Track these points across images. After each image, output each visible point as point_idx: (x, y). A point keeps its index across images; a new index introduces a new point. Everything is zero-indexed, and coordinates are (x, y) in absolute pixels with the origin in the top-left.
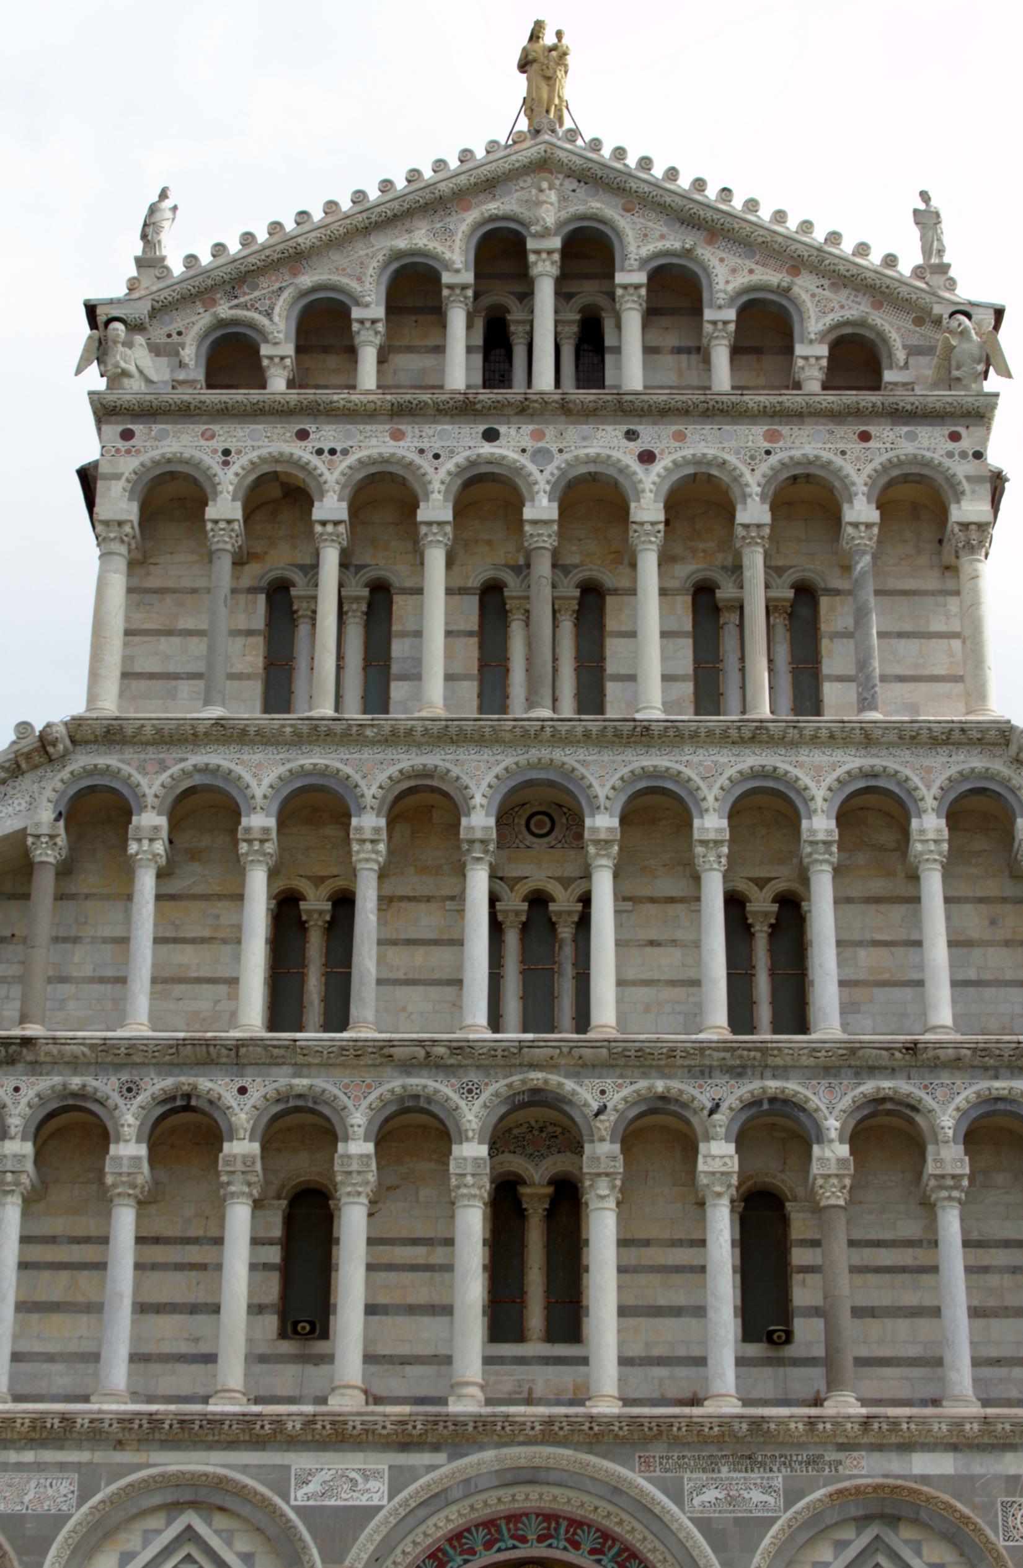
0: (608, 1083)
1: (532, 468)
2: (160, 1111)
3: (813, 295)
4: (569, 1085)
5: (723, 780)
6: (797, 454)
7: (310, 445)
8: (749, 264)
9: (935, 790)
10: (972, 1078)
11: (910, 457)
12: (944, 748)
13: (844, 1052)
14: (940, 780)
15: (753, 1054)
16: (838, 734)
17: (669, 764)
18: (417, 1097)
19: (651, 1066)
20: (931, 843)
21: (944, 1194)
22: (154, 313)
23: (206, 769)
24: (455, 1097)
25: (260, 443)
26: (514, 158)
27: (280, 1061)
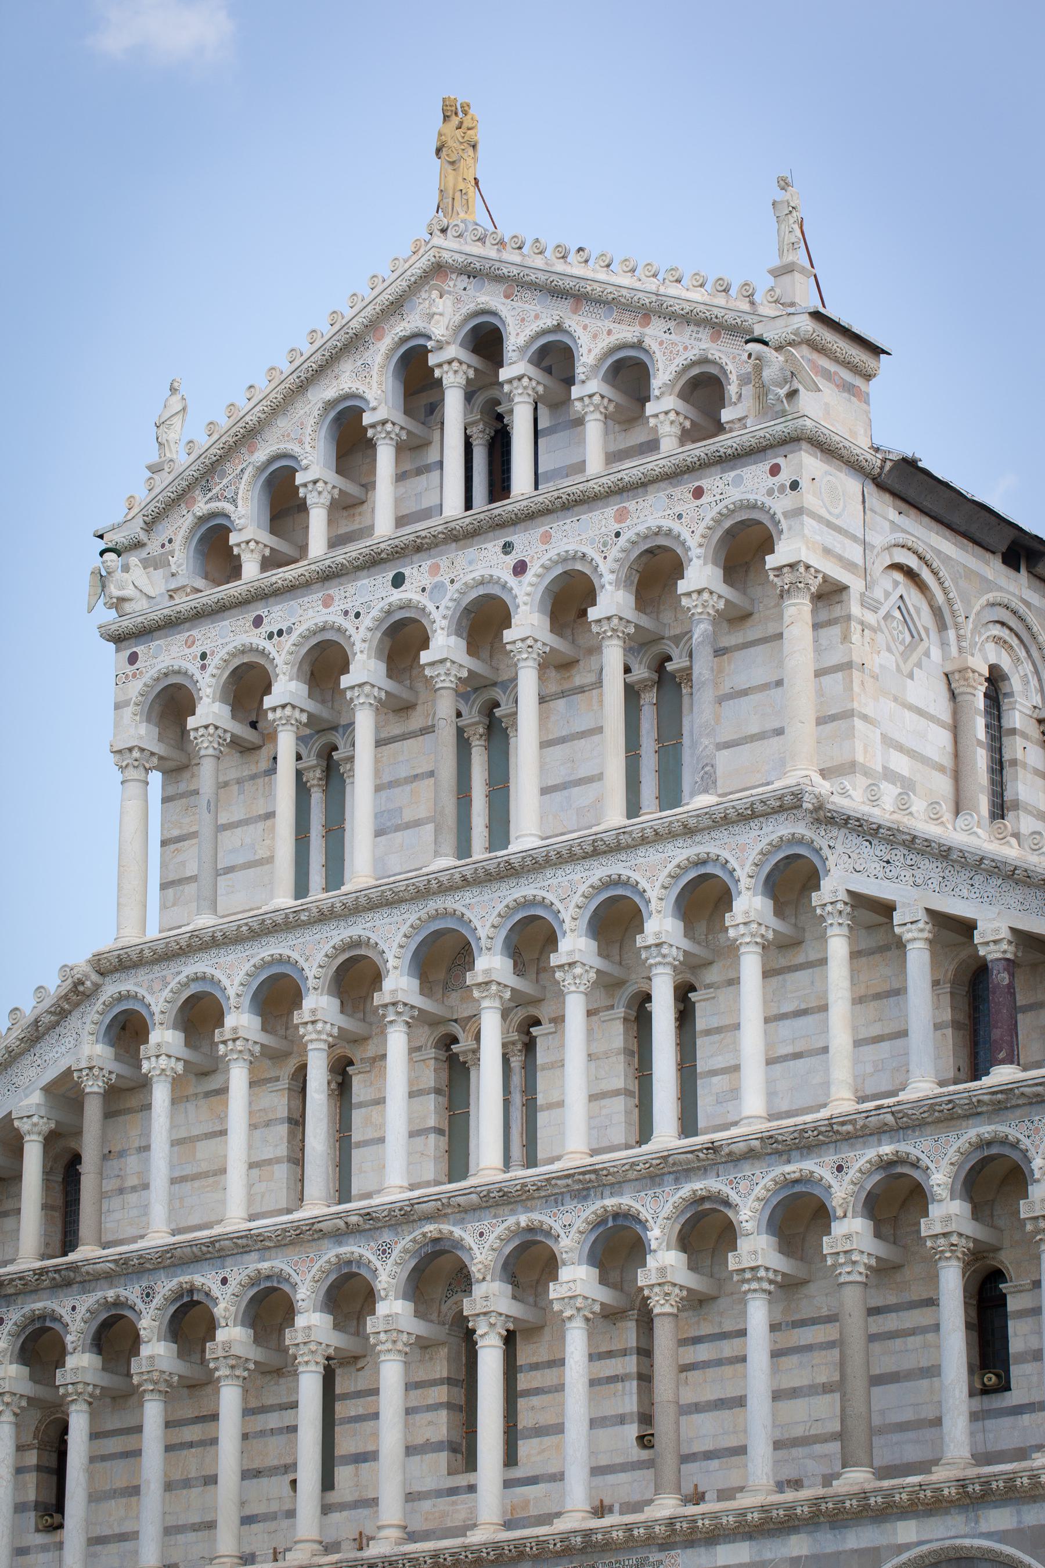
0: (484, 1224)
1: (430, 607)
2: (172, 1309)
3: (661, 343)
4: (457, 1232)
5: (578, 899)
6: (642, 529)
7: (263, 630)
8: (608, 324)
9: (749, 868)
10: (769, 1166)
11: (738, 504)
12: (756, 820)
13: (658, 1161)
14: (753, 855)
15: (587, 1177)
16: (661, 831)
17: (535, 892)
18: (349, 1262)
19: (516, 1202)
20: (741, 926)
21: (746, 1287)
22: (150, 526)
23: (196, 979)
24: (373, 1258)
25: (227, 640)
26: (409, 273)
27: (248, 1249)
